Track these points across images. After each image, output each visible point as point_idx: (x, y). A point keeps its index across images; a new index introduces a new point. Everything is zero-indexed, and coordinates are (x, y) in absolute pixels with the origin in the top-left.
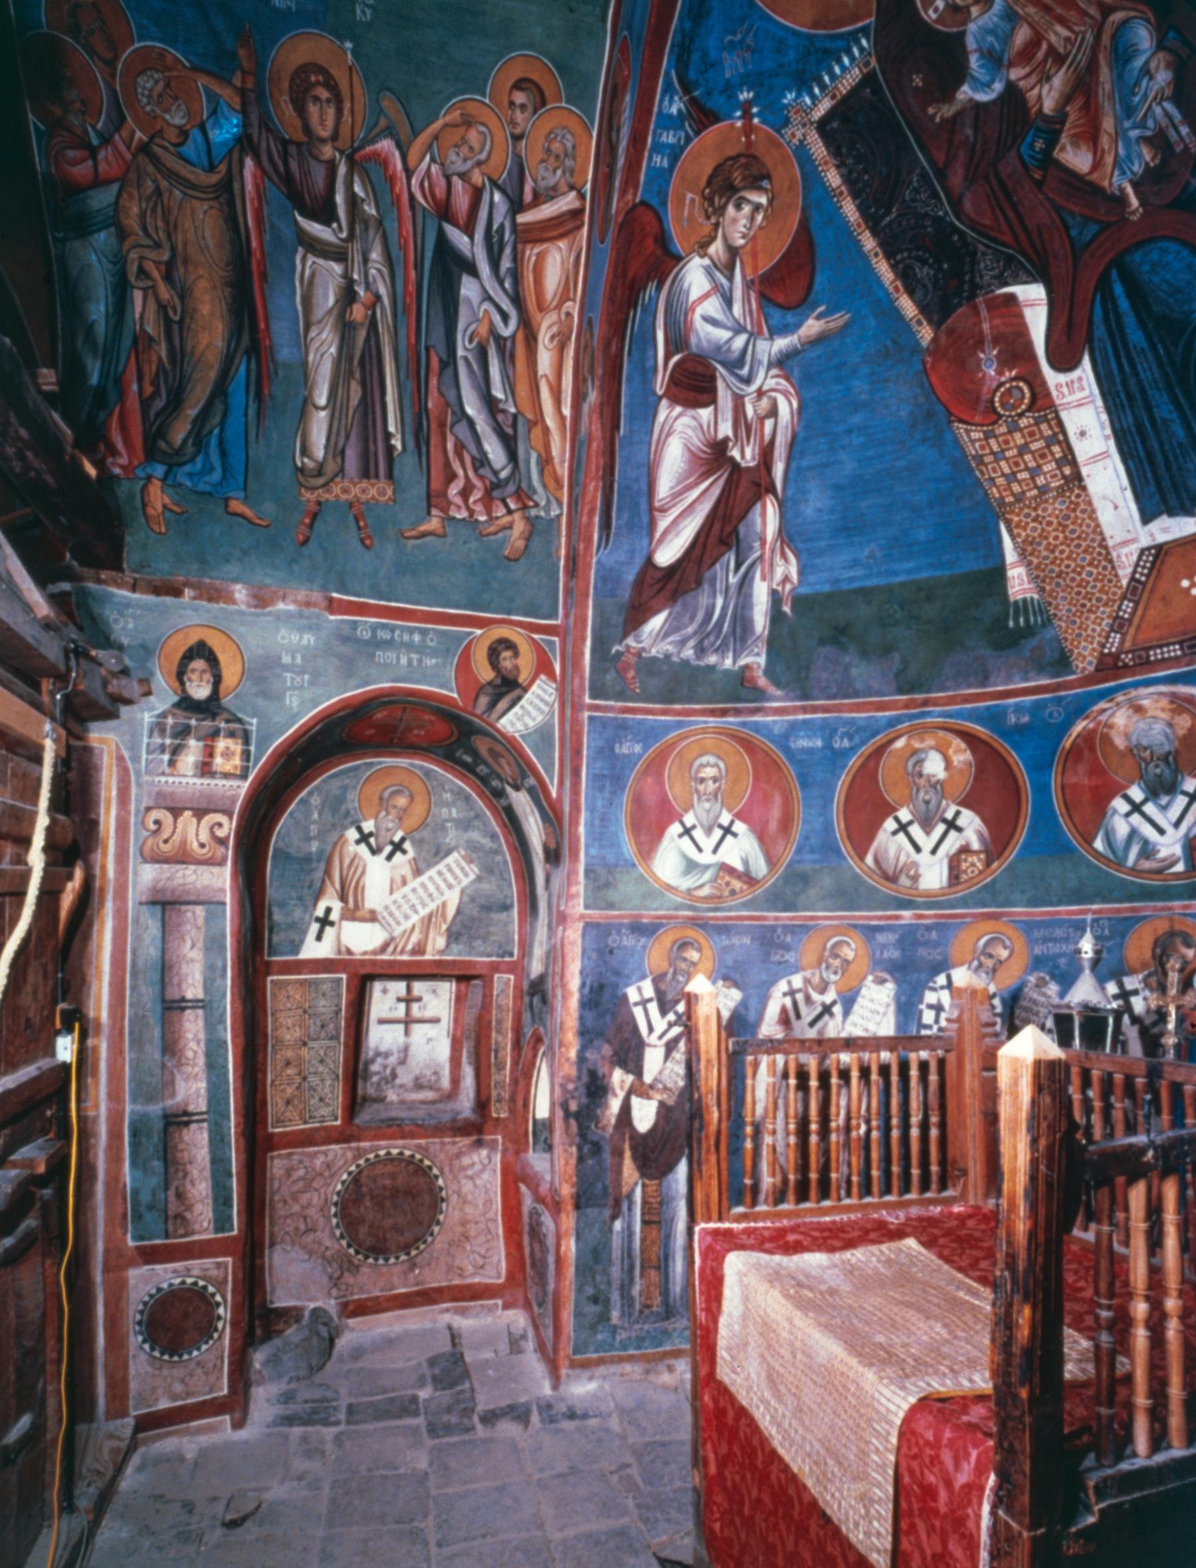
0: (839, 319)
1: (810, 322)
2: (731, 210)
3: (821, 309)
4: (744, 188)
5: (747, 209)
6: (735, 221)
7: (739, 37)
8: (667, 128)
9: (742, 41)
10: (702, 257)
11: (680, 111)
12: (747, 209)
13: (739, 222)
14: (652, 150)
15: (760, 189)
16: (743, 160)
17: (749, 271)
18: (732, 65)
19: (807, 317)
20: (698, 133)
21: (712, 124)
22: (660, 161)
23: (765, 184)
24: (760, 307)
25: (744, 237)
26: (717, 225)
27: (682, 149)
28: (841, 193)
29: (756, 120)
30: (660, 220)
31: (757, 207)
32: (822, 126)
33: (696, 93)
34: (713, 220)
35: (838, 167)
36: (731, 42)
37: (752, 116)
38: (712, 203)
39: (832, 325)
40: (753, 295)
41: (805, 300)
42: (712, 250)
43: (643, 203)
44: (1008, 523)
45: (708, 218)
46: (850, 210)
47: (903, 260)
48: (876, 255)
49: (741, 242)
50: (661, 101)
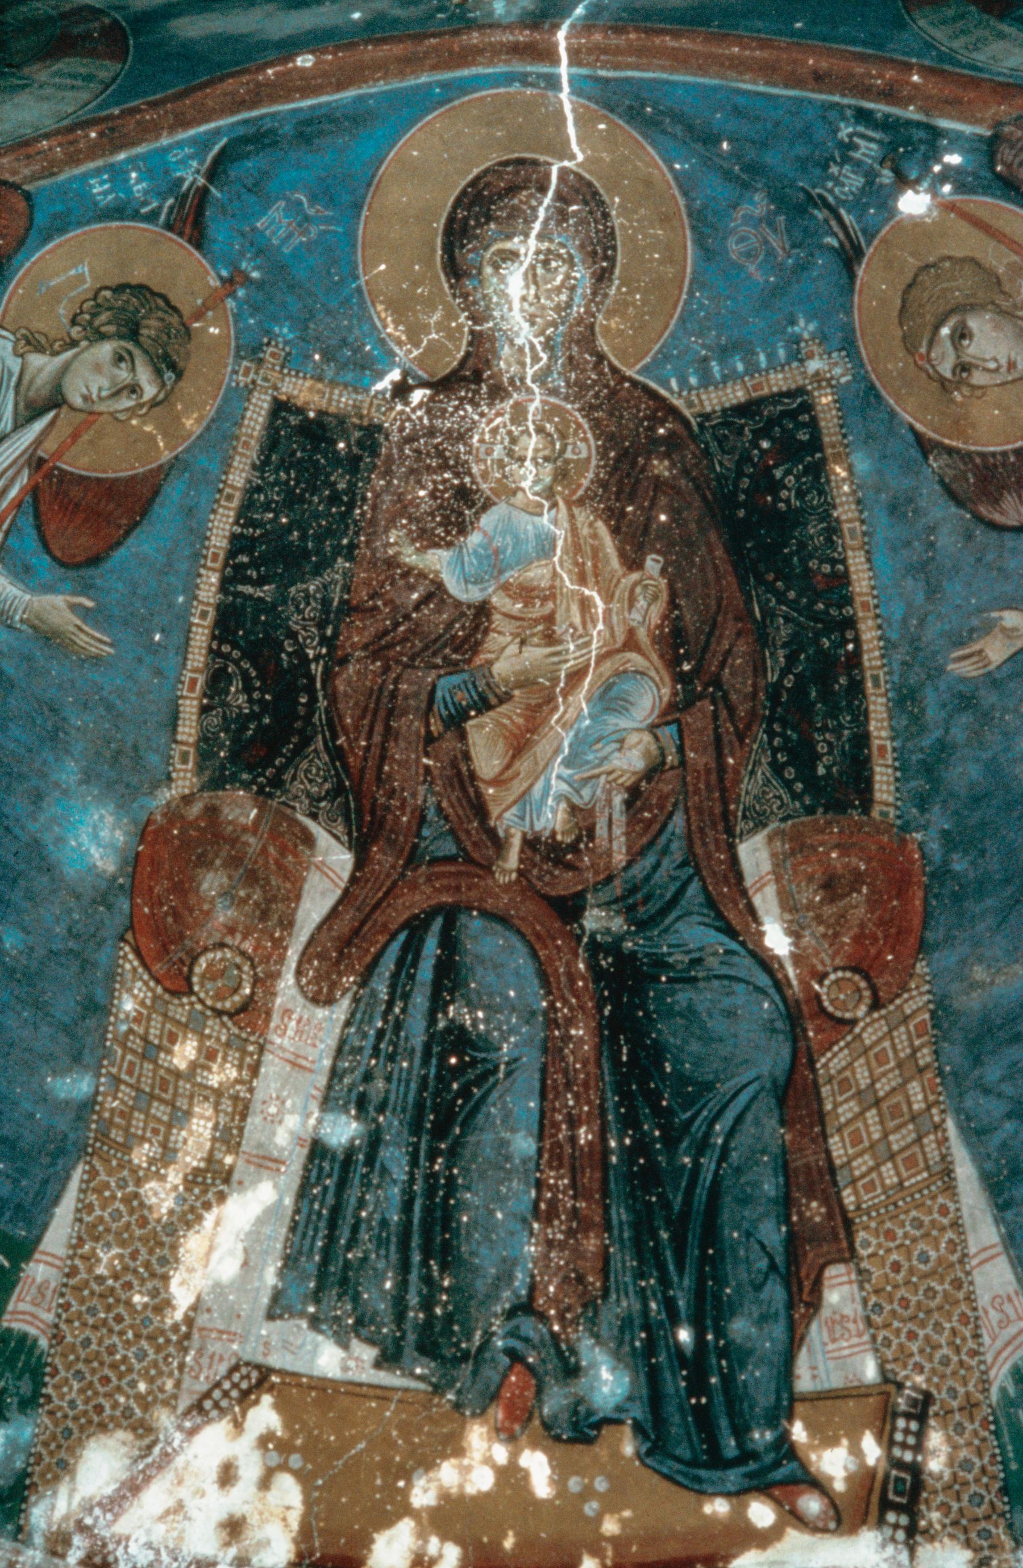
0: (92, 640)
1: (59, 600)
2: (106, 349)
3: (89, 604)
4: (146, 352)
5: (123, 374)
6: (98, 368)
7: (311, 212)
8: (148, 174)
9: (307, 219)
10: (16, 354)
11: (182, 180)
12: (123, 374)
13: (93, 373)
14: (111, 168)
15: (158, 372)
16: (174, 320)
17: (50, 445)
18: (274, 222)
19: (63, 593)
20: (169, 227)
21: (190, 241)
22: (98, 188)
23: (169, 376)
24: (18, 504)
25: (86, 398)
26: (74, 343)
27: (136, 216)
28: (230, 498)
29: (230, 303)
30: (21, 242)
31: (134, 389)
32: (280, 408)
33: (213, 189)
34: (75, 332)
35: (254, 467)
36: (299, 203)
37: (232, 294)
38: (94, 315)
39: (82, 640)
40: (24, 478)
41: (77, 566)
42: (36, 360)
43: (28, 196)
44: (93, 1173)
45: (74, 322)
46: (221, 528)
47: (226, 657)
48: (204, 615)
49: (78, 401)
50: (179, 144)
